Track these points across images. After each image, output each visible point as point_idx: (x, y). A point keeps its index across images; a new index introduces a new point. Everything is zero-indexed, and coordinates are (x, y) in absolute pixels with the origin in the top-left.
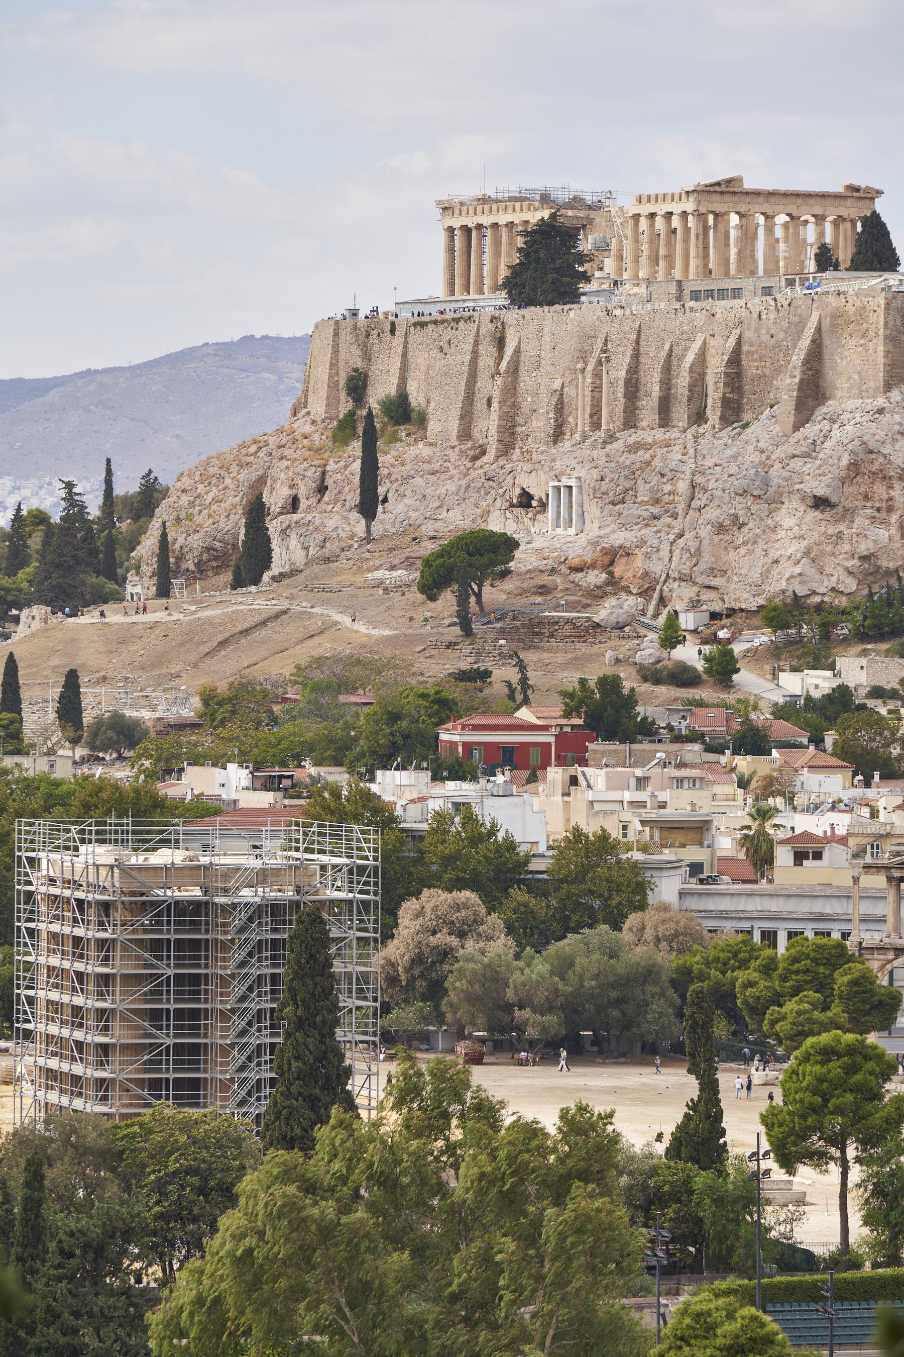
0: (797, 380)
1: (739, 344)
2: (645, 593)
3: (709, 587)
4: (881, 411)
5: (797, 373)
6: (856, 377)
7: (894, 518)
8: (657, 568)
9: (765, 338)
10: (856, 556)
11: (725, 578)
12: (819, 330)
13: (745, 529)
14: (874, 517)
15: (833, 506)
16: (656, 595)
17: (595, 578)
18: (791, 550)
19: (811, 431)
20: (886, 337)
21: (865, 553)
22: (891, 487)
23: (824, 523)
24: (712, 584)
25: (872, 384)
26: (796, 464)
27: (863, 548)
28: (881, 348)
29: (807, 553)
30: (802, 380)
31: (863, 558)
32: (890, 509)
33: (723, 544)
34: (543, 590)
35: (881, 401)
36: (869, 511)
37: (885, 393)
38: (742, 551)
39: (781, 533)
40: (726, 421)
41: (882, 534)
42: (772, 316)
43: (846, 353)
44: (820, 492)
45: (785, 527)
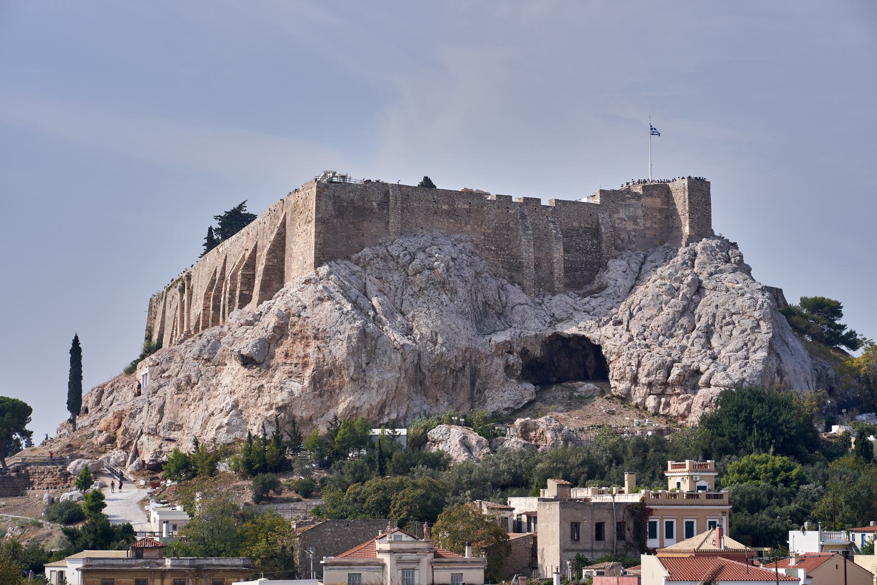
2: (125, 448)
3: (169, 440)
4: (307, 282)
6: (301, 258)
7: (308, 372)
8: (135, 426)
10: (274, 407)
11: (181, 431)
13: (195, 388)
14: (291, 372)
16: (132, 448)
18: (224, 405)
20: (318, 220)
21: (281, 404)
23: (250, 379)
24: (172, 437)
28: (314, 230)
29: (235, 405)
30: (266, 266)
31: (279, 409)
32: (305, 365)
33: (180, 402)
35: (311, 273)
36: (287, 368)
37: (316, 267)
38: (192, 407)
39: (220, 389)
41: (296, 387)
44: (245, 352)
45: (224, 385)
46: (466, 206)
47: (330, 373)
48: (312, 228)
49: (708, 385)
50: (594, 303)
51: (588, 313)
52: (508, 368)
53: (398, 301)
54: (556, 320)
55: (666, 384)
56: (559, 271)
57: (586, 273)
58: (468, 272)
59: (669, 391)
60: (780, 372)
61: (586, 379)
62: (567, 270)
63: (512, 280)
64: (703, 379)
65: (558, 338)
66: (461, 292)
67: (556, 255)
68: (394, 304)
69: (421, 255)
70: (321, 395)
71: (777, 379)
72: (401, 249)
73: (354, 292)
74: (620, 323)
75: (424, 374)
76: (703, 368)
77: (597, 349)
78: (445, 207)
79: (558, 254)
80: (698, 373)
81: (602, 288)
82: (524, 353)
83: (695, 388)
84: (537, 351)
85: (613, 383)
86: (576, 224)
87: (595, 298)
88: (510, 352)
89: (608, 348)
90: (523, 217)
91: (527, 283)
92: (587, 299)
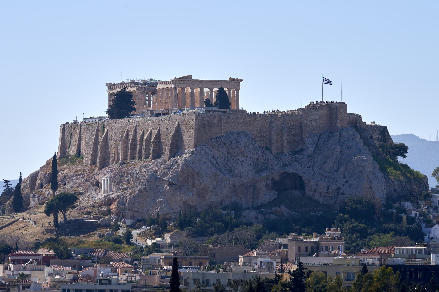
0: (170, 143)
1: (159, 130)
5: (170, 141)
9: (165, 129)
12: (178, 126)
15: (175, 185)
16: (121, 215)
17: (104, 209)
19: (173, 159)
20: (195, 129)
22: (194, 178)
25: (191, 144)
26: (165, 171)
27: (184, 199)
28: (194, 132)
34: (89, 213)
40: (154, 158)
42: (167, 122)
43: (185, 134)
46: (250, 120)
47: (203, 189)
48: (193, 132)
49: (343, 194)
50: (299, 157)
51: (297, 162)
52: (267, 185)
53: (226, 160)
54: (285, 165)
55: (327, 192)
56: (285, 144)
57: (295, 144)
58: (251, 147)
59: (328, 195)
60: (371, 188)
62: (288, 143)
63: (267, 149)
64: (341, 191)
65: (285, 172)
66: (249, 156)
67: (284, 138)
68: (224, 160)
69: (234, 142)
70: (199, 197)
71: (370, 190)
72: (226, 139)
73: (210, 157)
74: (310, 167)
75: (236, 189)
76: (341, 186)
77: (301, 178)
78: (242, 120)
79: (285, 137)
80: (339, 188)
81: (302, 150)
82: (273, 179)
83: (338, 194)
84: (277, 178)
85: (307, 192)
86: (292, 124)
87: (300, 155)
88: (267, 179)
89: (305, 178)
90: (271, 122)
91: (273, 149)
92: (296, 156)
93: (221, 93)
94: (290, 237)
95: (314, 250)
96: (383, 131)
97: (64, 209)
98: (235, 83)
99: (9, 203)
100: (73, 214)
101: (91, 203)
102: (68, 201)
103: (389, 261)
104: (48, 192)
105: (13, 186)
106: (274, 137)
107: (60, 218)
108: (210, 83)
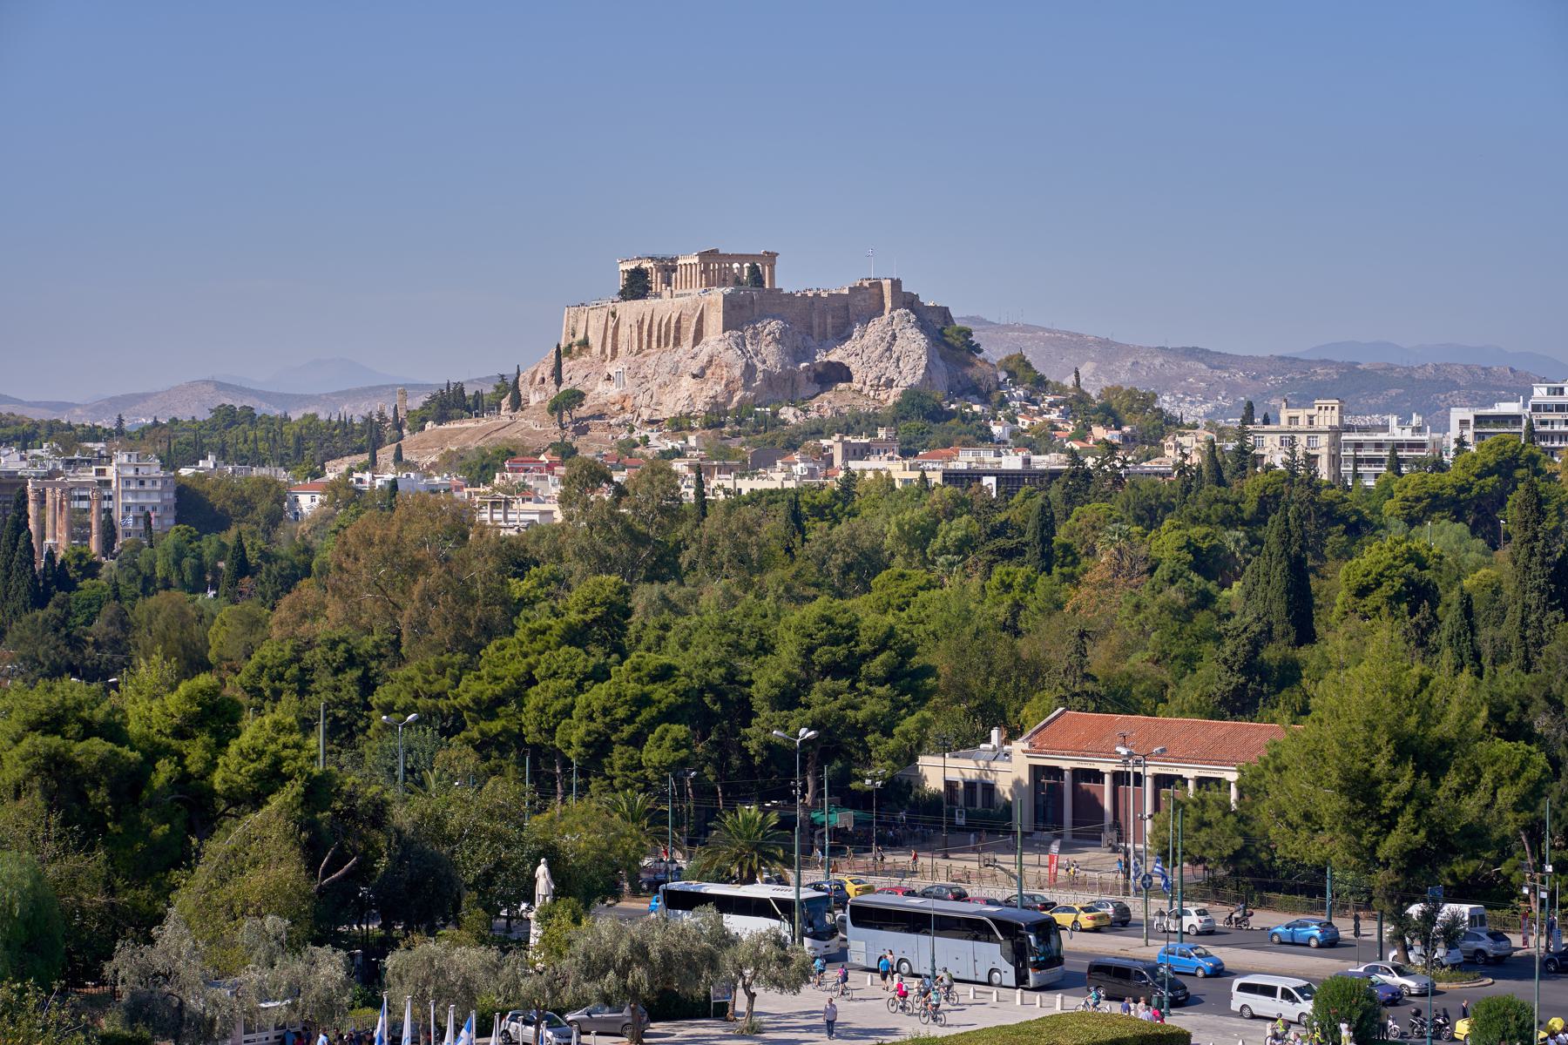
19: (697, 349)
61: (842, 381)
84: (820, 369)
89: (853, 368)
93: (754, 270)
94: (837, 437)
95: (863, 452)
96: (944, 312)
97: (569, 407)
98: (771, 257)
99: (505, 402)
100: (582, 411)
101: (602, 401)
102: (576, 397)
103: (951, 466)
104: (551, 387)
105: (510, 381)
106: (816, 321)
107: (566, 419)
108: (741, 258)
